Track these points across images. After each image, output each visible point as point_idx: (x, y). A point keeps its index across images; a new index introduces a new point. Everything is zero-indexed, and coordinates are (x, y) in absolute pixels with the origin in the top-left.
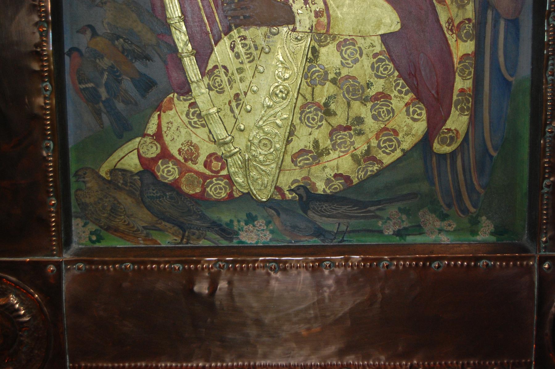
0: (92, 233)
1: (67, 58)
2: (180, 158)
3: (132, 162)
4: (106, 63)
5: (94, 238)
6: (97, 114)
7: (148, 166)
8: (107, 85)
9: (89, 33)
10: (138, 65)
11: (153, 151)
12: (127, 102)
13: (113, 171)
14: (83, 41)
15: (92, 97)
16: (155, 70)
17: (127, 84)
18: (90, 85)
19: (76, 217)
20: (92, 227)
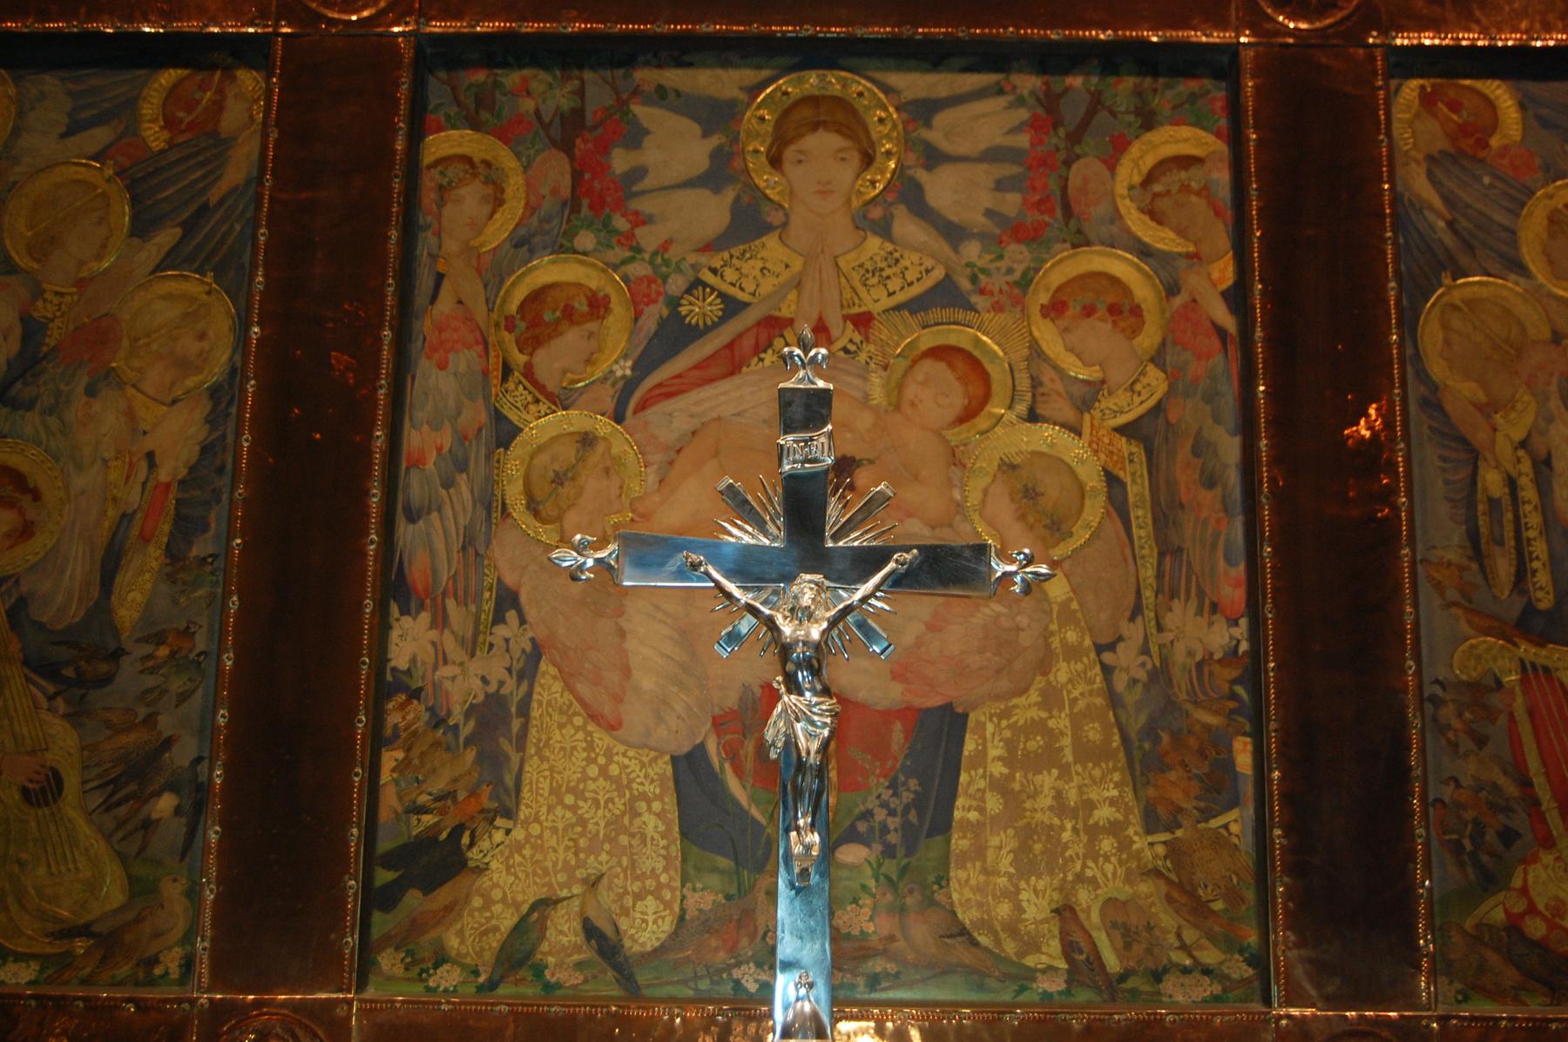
0: (1458, 992)
1: (1431, 810)
2: (1547, 913)
3: (1498, 916)
4: (1469, 815)
7: (1514, 925)
8: (1471, 836)
9: (1452, 785)
10: (1501, 816)
11: (1519, 907)
12: (1492, 854)
13: (1478, 926)
14: (1447, 793)
15: (1457, 848)
16: (1520, 821)
17: (1491, 836)
18: (1454, 837)
20: (1458, 985)
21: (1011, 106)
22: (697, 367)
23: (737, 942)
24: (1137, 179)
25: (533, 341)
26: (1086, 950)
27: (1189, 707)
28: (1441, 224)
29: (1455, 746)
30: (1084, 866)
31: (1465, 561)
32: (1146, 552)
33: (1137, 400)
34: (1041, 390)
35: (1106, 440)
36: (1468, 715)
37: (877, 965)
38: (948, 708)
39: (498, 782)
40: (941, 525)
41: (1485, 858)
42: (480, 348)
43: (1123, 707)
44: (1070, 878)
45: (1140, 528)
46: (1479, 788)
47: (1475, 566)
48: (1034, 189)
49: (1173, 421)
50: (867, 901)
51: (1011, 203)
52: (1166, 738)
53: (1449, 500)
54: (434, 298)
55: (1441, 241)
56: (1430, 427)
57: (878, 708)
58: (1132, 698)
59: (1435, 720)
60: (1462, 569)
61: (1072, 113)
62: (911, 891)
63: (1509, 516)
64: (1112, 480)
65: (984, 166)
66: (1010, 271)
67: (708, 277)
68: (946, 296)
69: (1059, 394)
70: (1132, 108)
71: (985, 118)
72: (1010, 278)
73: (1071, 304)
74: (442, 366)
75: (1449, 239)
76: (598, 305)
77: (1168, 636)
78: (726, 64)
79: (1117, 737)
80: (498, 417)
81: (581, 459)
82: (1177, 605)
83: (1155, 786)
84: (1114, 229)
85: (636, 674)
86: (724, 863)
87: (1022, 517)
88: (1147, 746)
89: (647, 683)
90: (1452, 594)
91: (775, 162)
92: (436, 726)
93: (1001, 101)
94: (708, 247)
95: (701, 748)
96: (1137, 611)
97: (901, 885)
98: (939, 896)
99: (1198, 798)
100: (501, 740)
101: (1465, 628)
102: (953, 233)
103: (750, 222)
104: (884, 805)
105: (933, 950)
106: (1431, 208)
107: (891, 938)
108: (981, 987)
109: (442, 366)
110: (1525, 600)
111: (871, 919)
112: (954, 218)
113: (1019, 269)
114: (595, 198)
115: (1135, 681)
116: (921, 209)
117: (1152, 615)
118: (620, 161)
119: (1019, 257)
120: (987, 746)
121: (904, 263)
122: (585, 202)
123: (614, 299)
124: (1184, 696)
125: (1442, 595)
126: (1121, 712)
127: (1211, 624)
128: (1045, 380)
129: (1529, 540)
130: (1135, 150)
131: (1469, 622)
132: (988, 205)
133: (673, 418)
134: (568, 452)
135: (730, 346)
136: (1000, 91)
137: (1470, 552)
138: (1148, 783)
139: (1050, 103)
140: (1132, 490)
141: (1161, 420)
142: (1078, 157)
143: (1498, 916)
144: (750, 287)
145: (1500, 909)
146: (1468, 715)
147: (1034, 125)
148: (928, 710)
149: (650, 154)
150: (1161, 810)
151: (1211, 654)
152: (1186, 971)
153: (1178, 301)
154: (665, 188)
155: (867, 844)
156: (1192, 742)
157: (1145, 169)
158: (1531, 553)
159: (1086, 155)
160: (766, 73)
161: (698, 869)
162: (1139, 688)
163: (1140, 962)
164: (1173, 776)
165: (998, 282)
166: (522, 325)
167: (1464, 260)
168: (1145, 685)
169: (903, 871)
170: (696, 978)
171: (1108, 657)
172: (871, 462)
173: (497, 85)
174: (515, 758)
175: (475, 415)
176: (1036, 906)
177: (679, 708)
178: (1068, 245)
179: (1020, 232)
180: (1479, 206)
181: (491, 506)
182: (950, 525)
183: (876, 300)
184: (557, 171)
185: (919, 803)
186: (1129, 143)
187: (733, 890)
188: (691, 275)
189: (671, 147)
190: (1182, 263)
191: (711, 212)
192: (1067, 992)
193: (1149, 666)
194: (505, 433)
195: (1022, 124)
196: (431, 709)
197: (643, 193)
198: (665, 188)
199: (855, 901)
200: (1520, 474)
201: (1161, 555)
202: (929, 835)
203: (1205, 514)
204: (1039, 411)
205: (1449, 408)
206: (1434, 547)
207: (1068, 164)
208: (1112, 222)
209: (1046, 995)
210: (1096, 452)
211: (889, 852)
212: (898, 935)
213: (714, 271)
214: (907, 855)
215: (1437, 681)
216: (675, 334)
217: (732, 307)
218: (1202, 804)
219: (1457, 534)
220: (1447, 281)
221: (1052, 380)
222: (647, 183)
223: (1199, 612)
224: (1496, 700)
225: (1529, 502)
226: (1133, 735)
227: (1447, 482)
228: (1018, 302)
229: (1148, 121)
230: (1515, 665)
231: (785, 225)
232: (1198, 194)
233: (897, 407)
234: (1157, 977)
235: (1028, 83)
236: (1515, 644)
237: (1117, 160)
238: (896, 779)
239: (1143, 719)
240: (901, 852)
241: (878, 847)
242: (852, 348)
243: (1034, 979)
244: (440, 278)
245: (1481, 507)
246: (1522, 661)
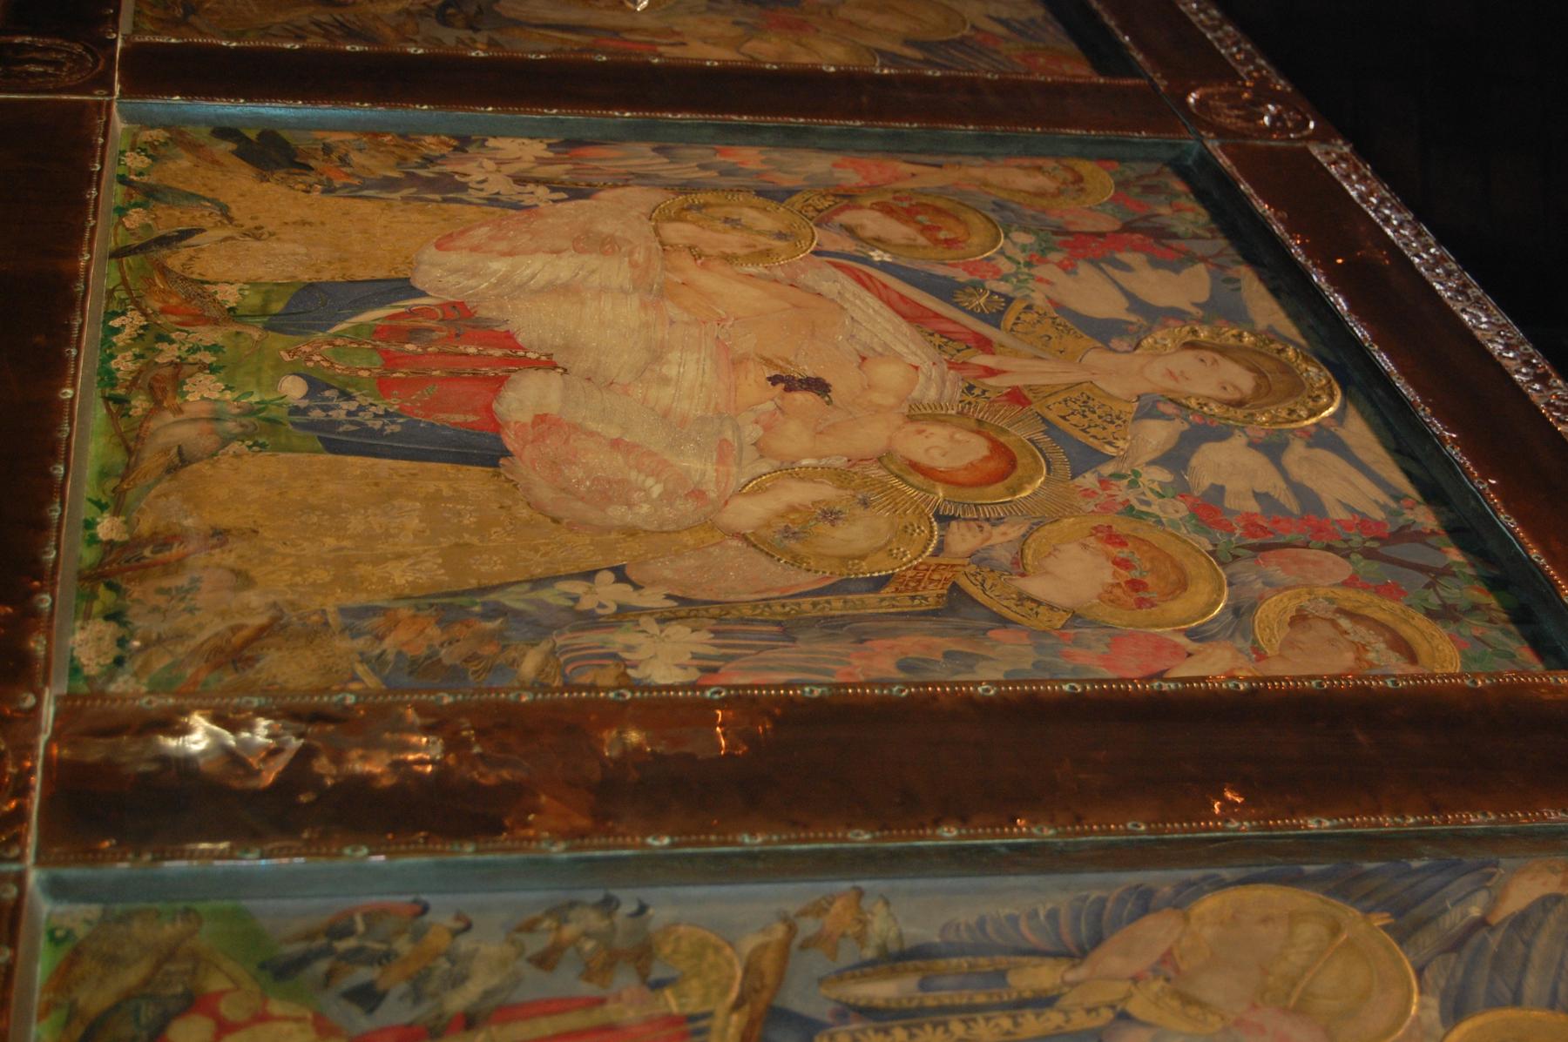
4: (403, 946)
5: (59, 933)
6: (310, 936)
8: (359, 951)
10: (403, 987)
12: (330, 976)
17: (363, 974)
19: (104, 911)
21: (1383, 507)
22: (902, 297)
23: (172, 313)
24: (1348, 606)
26: (159, 556)
27: (545, 646)
28: (1475, 912)
29: (530, 927)
30: (285, 556)
31: (874, 941)
32: (778, 609)
33: (1011, 604)
34: (987, 526)
35: (936, 577)
36: (589, 945)
37: (140, 404)
38: (506, 453)
39: (361, 188)
40: (760, 450)
41: (322, 966)
42: (866, 183)
43: (532, 590)
44: (268, 544)
45: (814, 605)
46: (451, 957)
47: (869, 953)
48: (1277, 522)
49: (990, 634)
50: (228, 395)
52: (491, 625)
53: (981, 923)
54: (907, 162)
55: (1445, 910)
56: (1102, 902)
57: (495, 405)
58: (548, 595)
59: (572, 905)
60: (861, 938)
62: (242, 426)
63: (980, 999)
64: (879, 583)
65: (1282, 484)
66: (1148, 503)
67: (1018, 306)
69: (988, 539)
70: (1449, 602)
72: (1134, 502)
73: (1126, 550)
74: (835, 165)
75: (1454, 919)
77: (654, 628)
78: (1295, 317)
79: (485, 582)
80: (791, 192)
81: (760, 233)
82: (705, 636)
83: (415, 616)
84: (1258, 585)
85: (509, 260)
86: (277, 307)
87: (793, 509)
88: (477, 609)
89: (499, 266)
90: (808, 927)
91: (1191, 346)
92: (423, 158)
93: (1383, 498)
94: (1058, 307)
95: (423, 294)
96: (683, 601)
97: (253, 419)
98: (236, 446)
99: (399, 654)
100: (414, 190)
101: (749, 943)
104: (361, 408)
105: (161, 440)
106: (1495, 901)
107: (180, 411)
108: (104, 474)
109: (835, 165)
110: (827, 1019)
111: (203, 398)
112: (1194, 462)
113: (1154, 509)
114: (1080, 246)
115: (576, 599)
117: (683, 614)
119: (1171, 510)
121: (1111, 428)
122: (1071, 239)
123: (961, 252)
124: (560, 642)
125: (803, 913)
126: (527, 587)
127: (684, 667)
128: (1002, 528)
129: (945, 1024)
130: (1388, 604)
131: (764, 947)
132: (1228, 487)
133: (833, 283)
135: (937, 316)
136: (1397, 497)
137: (893, 947)
138: (419, 609)
140: (871, 598)
141: (987, 624)
142: (1347, 557)
143: (216, 983)
144: (1019, 328)
145: (227, 985)
146: (589, 945)
147: (1364, 523)
148: (499, 439)
150: (377, 621)
151: (634, 667)
152: (121, 642)
153: (1182, 640)
154: (1115, 282)
155: (304, 397)
156: (488, 650)
157: (1367, 612)
158: (921, 1026)
159: (1352, 563)
160: (1303, 342)
161: (267, 292)
162: (570, 603)
163: (138, 601)
164: (434, 632)
165: (1121, 491)
166: (905, 204)
167: (1427, 940)
168: (571, 608)
169: (273, 422)
170: (129, 291)
171: (609, 576)
172: (829, 403)
173: (1178, 196)
174: (397, 196)
175: (787, 181)
177: (472, 282)
178: (1210, 548)
180: (1536, 958)
182: (762, 457)
185: (364, 430)
186: (1396, 599)
187: (239, 312)
188: (1018, 294)
190: (1246, 646)
192: (93, 540)
193: (600, 611)
195: (1363, 514)
196: (443, 156)
197: (1101, 269)
198: (1115, 282)
199: (228, 388)
200: (1066, 1012)
201: (779, 623)
202: (320, 438)
203: (856, 662)
204: (954, 524)
205: (1149, 921)
206: (887, 903)
207: (1329, 548)
208: (1265, 584)
209: (90, 525)
210: (915, 568)
211: (295, 410)
212: (181, 417)
213: (1029, 308)
214: (293, 424)
215: (642, 909)
218: (390, 657)
219: (921, 930)
220: (1380, 920)
221: (1004, 534)
222: (1118, 274)
223: (695, 656)
224: (625, 981)
225: (1016, 1024)
226: (492, 597)
227: (1013, 920)
228: (1105, 509)
229: (1444, 614)
230: (693, 1005)
231: (1115, 351)
232: (1358, 659)
233: (911, 418)
234: (114, 616)
236: (737, 1006)
237: (1365, 587)
238: (400, 416)
239: (519, 606)
240: (296, 419)
241: (304, 404)
242: (977, 392)
243: (116, 513)
244: (939, 166)
245: (982, 961)
246: (708, 1015)
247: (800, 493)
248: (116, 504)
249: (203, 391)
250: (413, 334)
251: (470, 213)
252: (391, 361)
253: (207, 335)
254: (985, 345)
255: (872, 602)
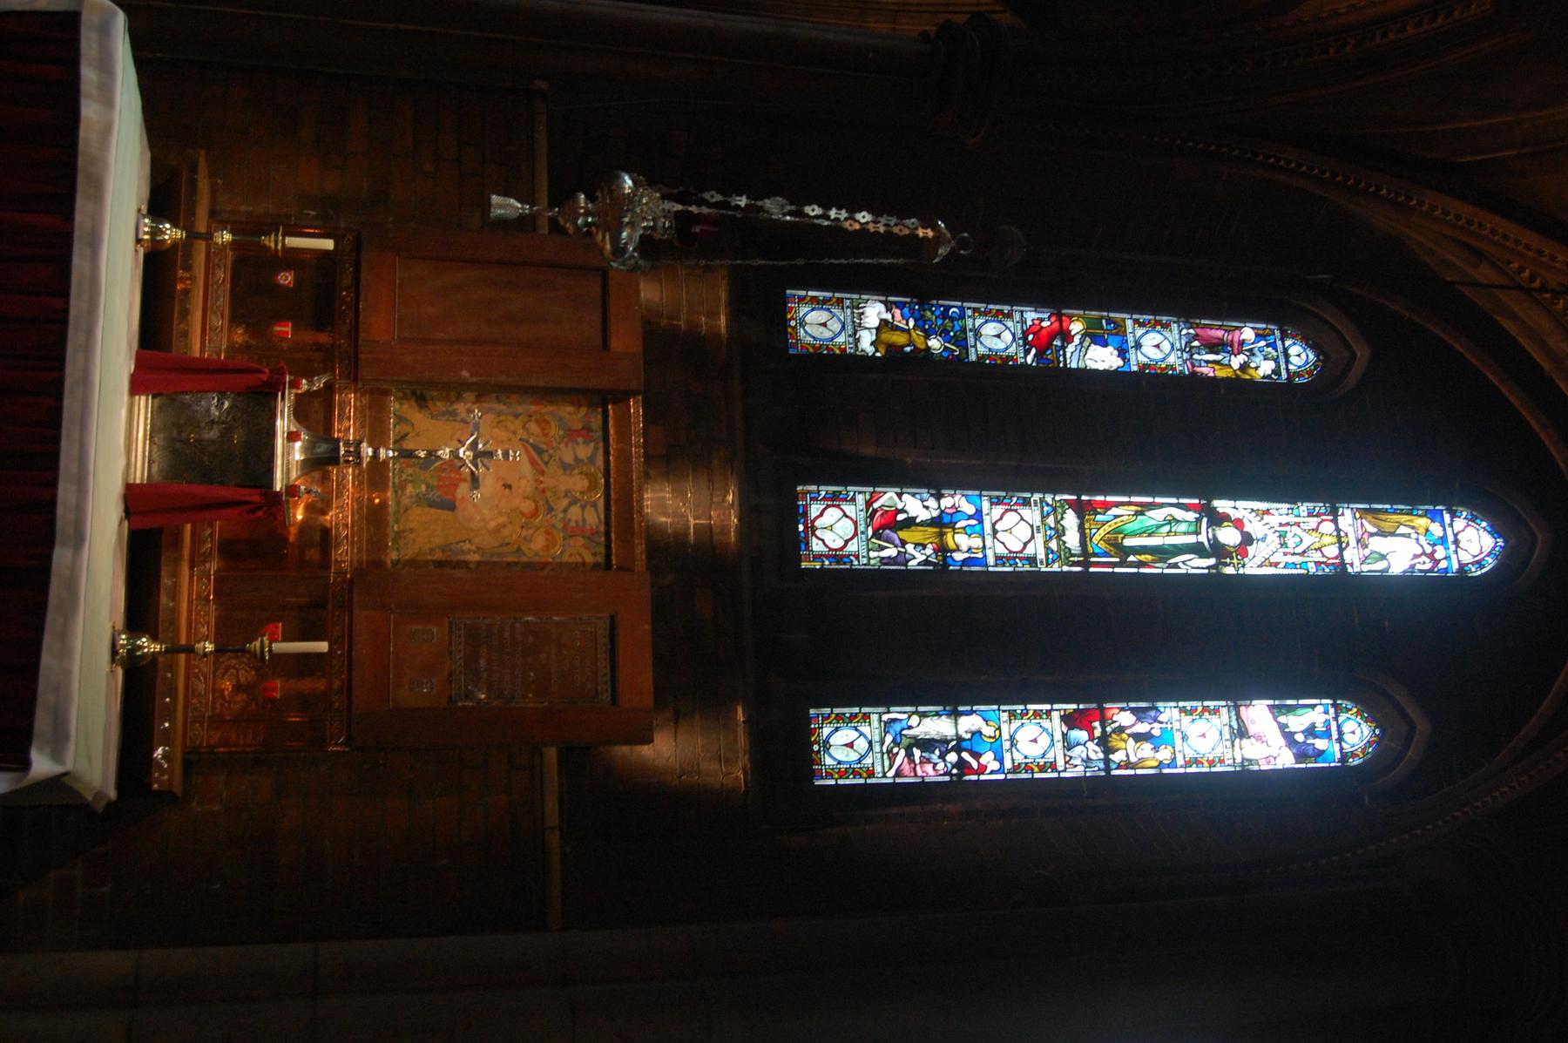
25: (537, 421)
51: (573, 524)
61: (596, 538)
68: (550, 509)
71: (594, 519)
76: (546, 435)
94: (561, 461)
102: (565, 511)
103: (566, 468)
114: (571, 435)
116: (570, 504)
118: (580, 440)
120: (447, 514)
134: (512, 427)
139: (596, 533)
149: (582, 446)
176: (412, 525)
179: (566, 526)
181: (499, 414)
183: (549, 494)
184: (578, 426)
189: (584, 451)
191: (569, 459)
194: (516, 416)
216: (540, 452)
217: (546, 464)
235: (602, 528)
247: (502, 520)
248: (397, 521)
249: (409, 489)
250: (444, 470)
251: (457, 425)
252: (441, 479)
253: (410, 471)
254: (542, 472)
255: (506, 549)
